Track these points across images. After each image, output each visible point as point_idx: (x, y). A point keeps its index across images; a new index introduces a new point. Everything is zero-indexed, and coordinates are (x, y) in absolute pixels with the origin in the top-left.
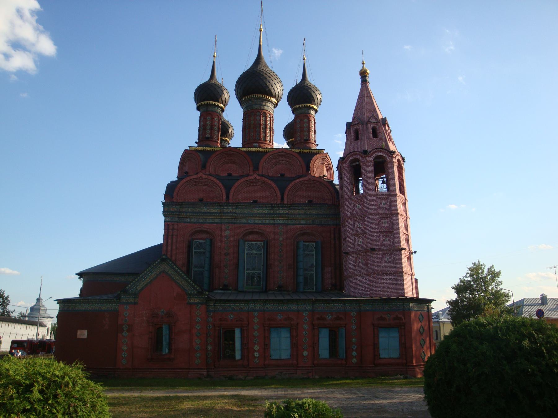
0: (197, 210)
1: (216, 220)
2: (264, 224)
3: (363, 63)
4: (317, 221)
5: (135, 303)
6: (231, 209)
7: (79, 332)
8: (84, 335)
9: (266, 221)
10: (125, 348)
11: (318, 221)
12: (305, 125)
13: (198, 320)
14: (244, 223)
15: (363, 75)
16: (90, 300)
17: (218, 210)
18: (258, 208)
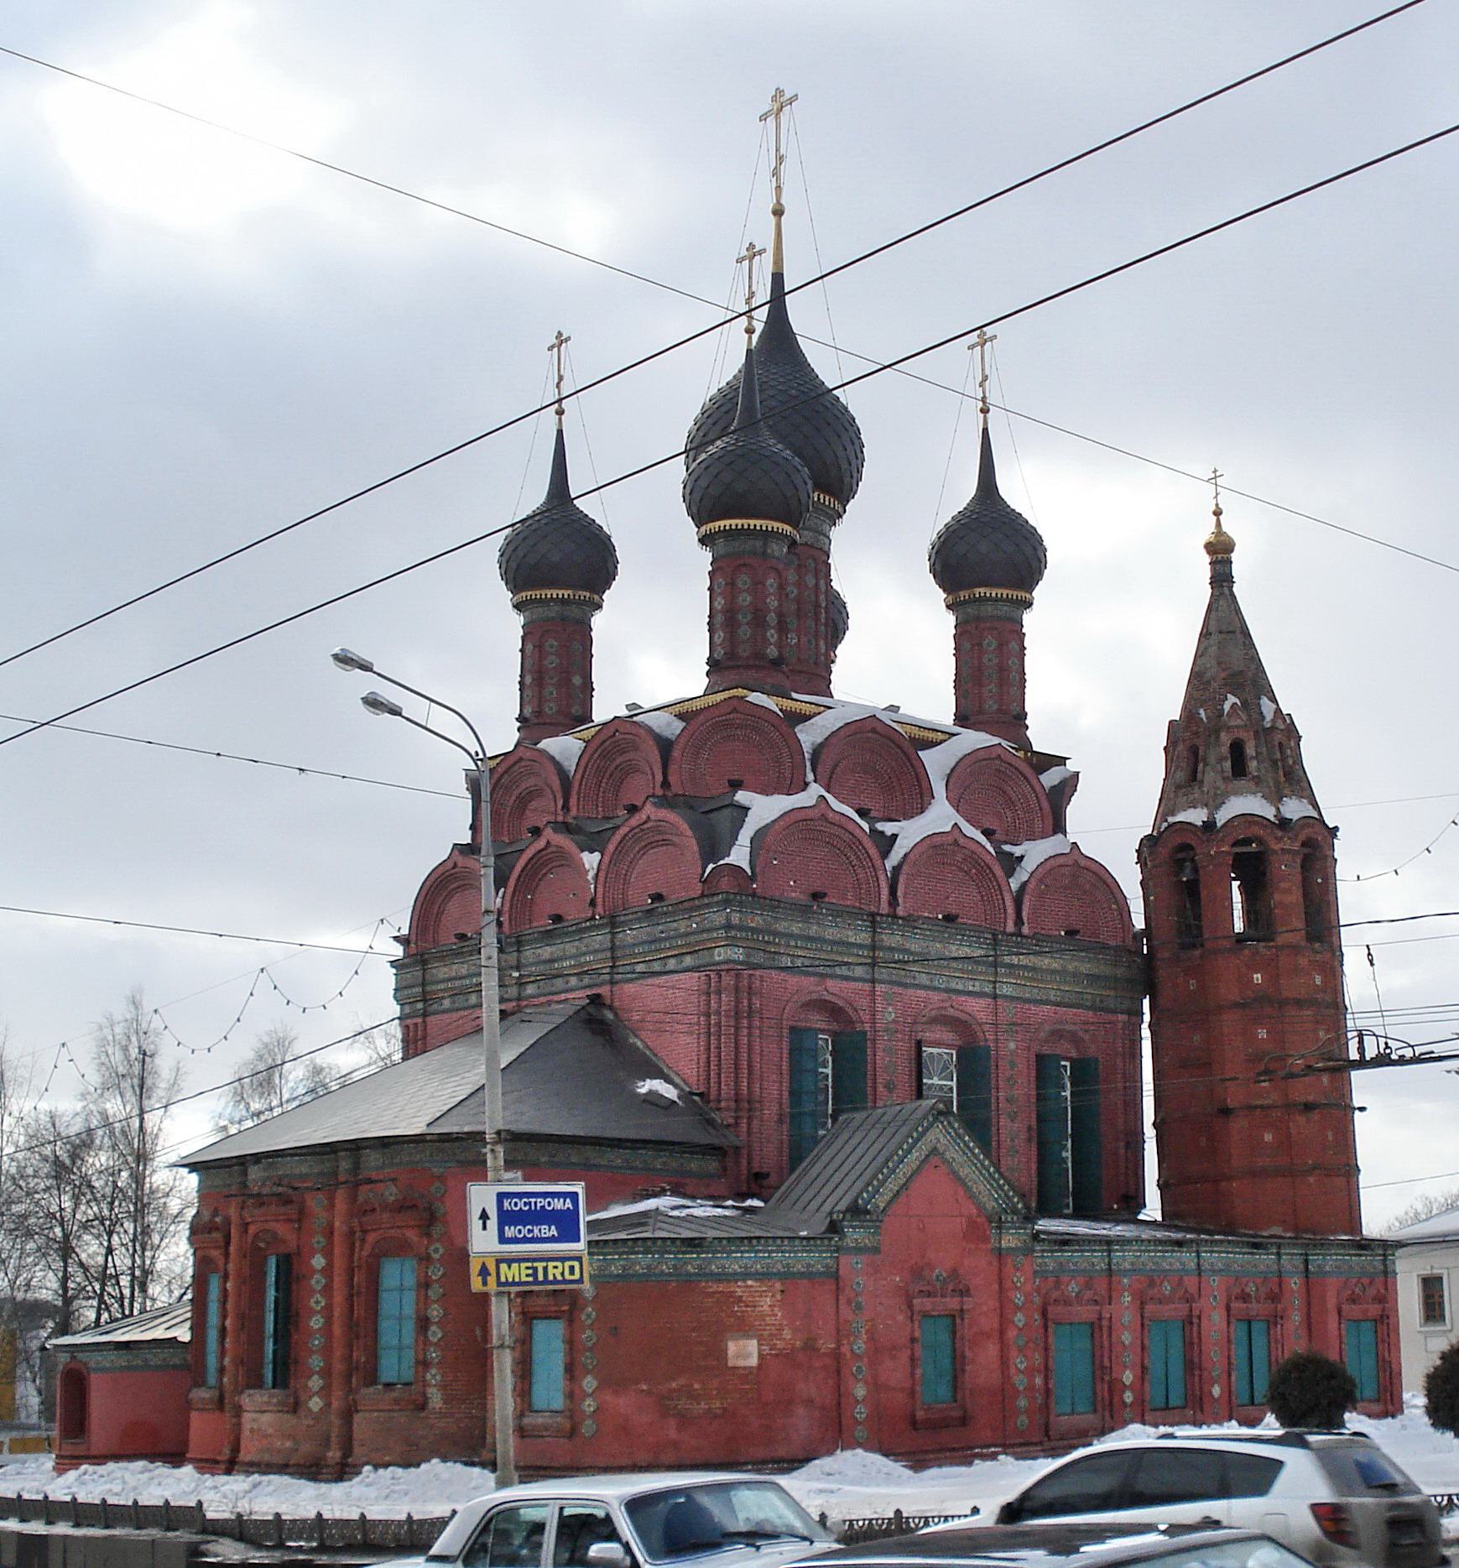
0: (814, 930)
1: (859, 971)
2: (969, 993)
3: (1218, 513)
4: (1085, 996)
5: (876, 1250)
6: (898, 938)
7: (732, 1347)
8: (749, 1355)
9: (974, 986)
10: (860, 1392)
11: (1089, 997)
12: (1012, 662)
13: (1019, 1298)
14: (925, 987)
15: (1220, 551)
16: (763, 1241)
17: (863, 937)
18: (959, 940)
